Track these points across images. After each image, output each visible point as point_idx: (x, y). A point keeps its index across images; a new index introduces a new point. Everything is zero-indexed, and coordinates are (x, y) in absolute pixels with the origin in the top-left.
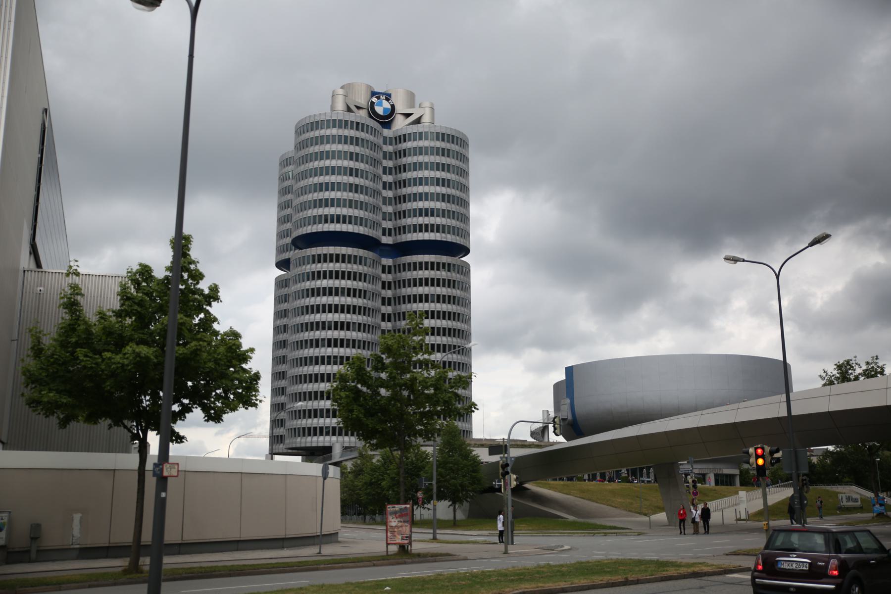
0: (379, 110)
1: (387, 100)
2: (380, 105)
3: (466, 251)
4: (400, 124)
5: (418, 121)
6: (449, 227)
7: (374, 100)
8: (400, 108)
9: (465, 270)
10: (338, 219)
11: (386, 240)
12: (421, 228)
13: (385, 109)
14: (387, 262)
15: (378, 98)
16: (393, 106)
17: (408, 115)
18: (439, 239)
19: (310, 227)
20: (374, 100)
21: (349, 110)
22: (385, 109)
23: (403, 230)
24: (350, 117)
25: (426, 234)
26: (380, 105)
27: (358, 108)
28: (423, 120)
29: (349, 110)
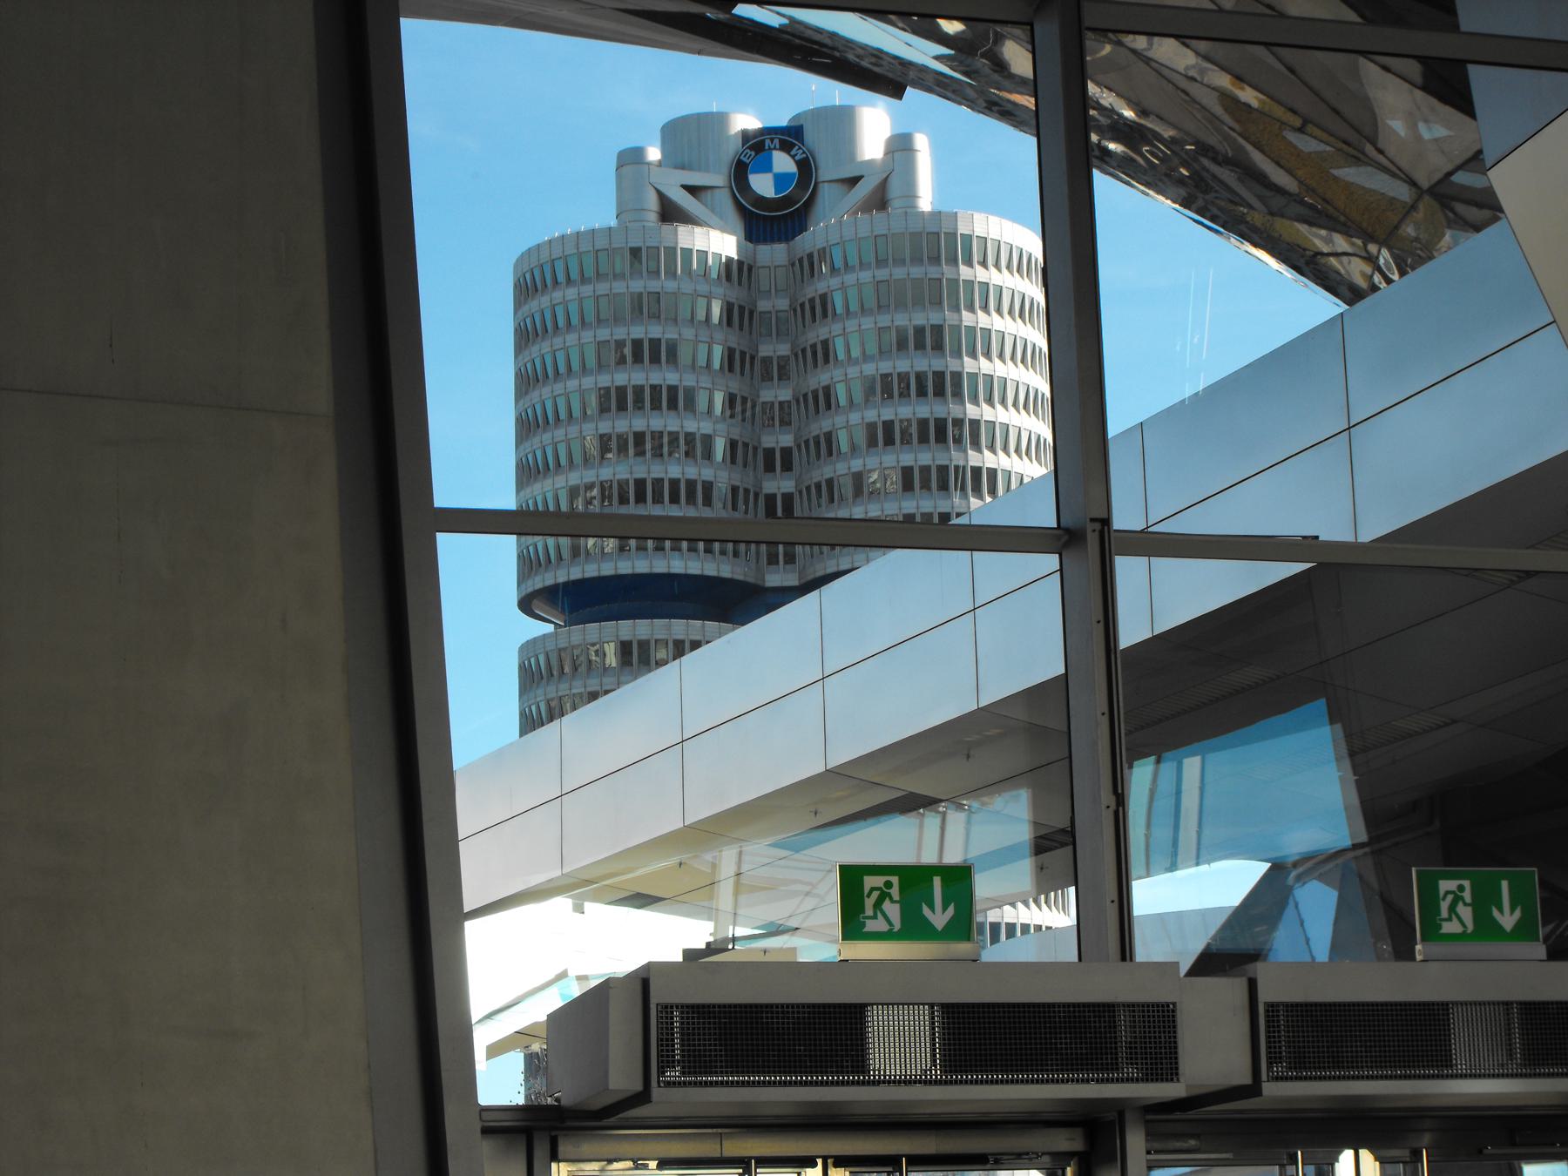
0: (762, 185)
1: (786, 147)
2: (767, 167)
8: (827, 170)
13: (780, 180)
16: (806, 167)
17: (853, 181)
22: (780, 180)
26: (767, 167)
27: (693, 190)
28: (894, 190)
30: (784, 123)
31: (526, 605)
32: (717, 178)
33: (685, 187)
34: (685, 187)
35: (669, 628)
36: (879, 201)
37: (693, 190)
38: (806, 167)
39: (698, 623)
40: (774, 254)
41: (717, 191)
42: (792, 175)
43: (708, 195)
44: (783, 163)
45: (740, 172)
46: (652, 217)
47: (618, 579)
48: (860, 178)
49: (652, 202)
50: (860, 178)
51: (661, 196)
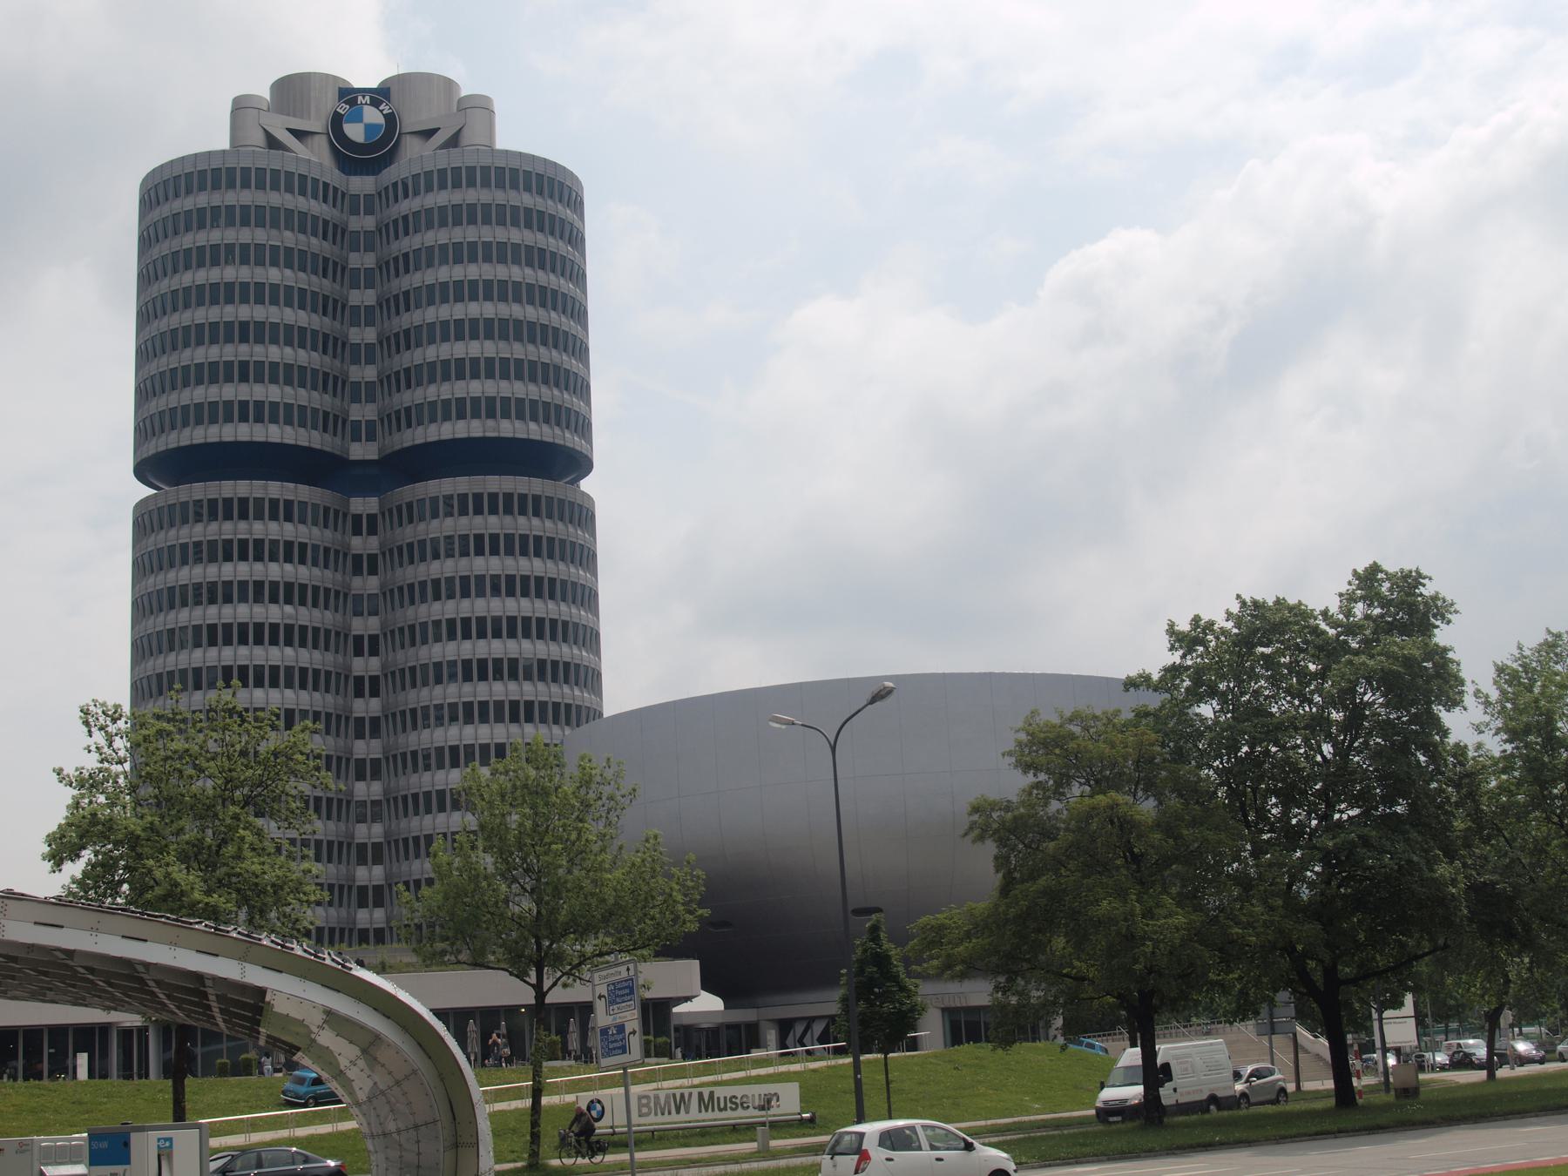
0: (355, 132)
1: (375, 103)
3: (580, 464)
4: (415, 156)
5: (454, 141)
6: (533, 403)
7: (343, 109)
8: (412, 120)
9: (582, 514)
10: (245, 411)
11: (361, 451)
14: (364, 505)
15: (352, 102)
17: (428, 134)
18: (479, 434)
19: (174, 435)
20: (343, 109)
21: (273, 143)
22: (370, 128)
24: (274, 161)
25: (461, 424)
27: (299, 135)
28: (466, 139)
30: (373, 84)
31: (144, 471)
32: (316, 123)
33: (291, 131)
34: (291, 131)
35: (266, 488)
36: (454, 141)
37: (299, 135)
38: (391, 119)
39: (291, 485)
40: (362, 185)
41: (317, 137)
42: (379, 126)
43: (309, 140)
44: (373, 116)
45: (337, 121)
47: (221, 445)
48: (435, 131)
49: (259, 139)
50: (435, 131)
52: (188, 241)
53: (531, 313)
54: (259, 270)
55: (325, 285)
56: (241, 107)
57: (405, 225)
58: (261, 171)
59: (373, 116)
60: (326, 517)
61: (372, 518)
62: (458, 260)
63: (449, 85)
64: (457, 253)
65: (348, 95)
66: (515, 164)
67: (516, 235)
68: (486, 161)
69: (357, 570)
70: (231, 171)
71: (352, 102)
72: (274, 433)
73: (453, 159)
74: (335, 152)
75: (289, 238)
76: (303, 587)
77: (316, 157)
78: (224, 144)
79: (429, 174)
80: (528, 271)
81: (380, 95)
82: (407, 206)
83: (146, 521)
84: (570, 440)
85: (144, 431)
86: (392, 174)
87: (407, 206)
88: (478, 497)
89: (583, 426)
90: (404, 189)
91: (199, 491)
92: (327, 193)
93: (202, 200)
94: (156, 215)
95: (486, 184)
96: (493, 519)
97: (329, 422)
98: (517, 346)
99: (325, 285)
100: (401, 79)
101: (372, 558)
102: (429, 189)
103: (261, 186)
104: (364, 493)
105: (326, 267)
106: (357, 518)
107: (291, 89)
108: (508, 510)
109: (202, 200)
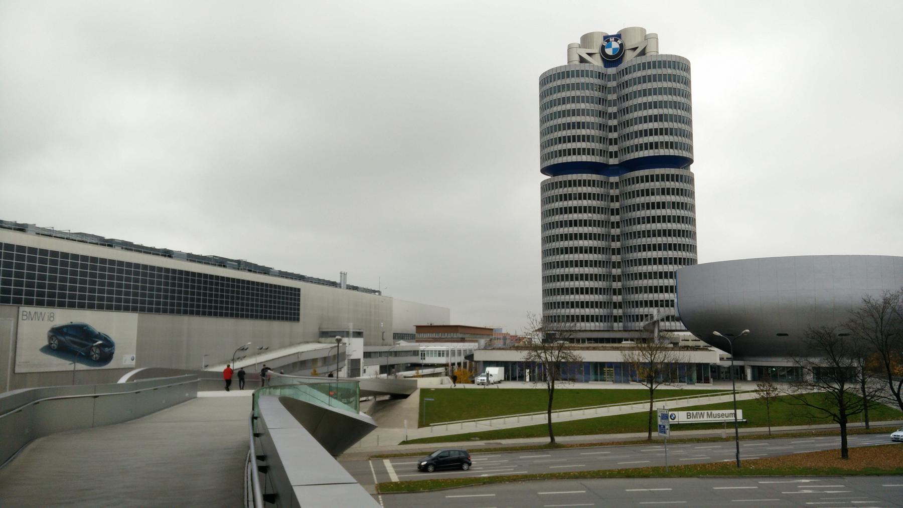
0: (609, 51)
1: (616, 40)
2: (610, 46)
3: (689, 161)
4: (630, 58)
5: (643, 53)
7: (605, 44)
8: (629, 45)
9: (690, 180)
11: (613, 161)
12: (640, 147)
14: (614, 179)
17: (635, 49)
21: (582, 60)
23: (628, 150)
26: (610, 46)
27: (590, 54)
28: (647, 50)
29: (582, 60)
30: (615, 33)
32: (596, 50)
36: (643, 53)
37: (590, 54)
38: (621, 45)
40: (612, 71)
45: (603, 48)
46: (577, 63)
47: (567, 163)
49: (577, 58)
51: (580, 56)
52: (555, 96)
53: (670, 111)
54: (578, 105)
55: (600, 107)
56: (570, 48)
57: (626, 84)
58: (578, 71)
59: (615, 45)
60: (601, 184)
61: (617, 183)
62: (645, 95)
63: (643, 30)
64: (645, 93)
65: (607, 38)
66: (664, 59)
67: (666, 84)
68: (654, 59)
69: (612, 201)
70: (568, 72)
71: (608, 41)
72: (584, 158)
73: (643, 59)
74: (603, 60)
75: (587, 93)
76: (594, 207)
77: (597, 63)
78: (565, 62)
79: (634, 66)
80: (670, 96)
81: (618, 37)
82: (627, 78)
83: (545, 187)
84: (685, 154)
85: (543, 158)
86: (622, 66)
87: (627, 78)
88: (652, 176)
89: (690, 148)
90: (626, 71)
91: (561, 178)
92: (600, 75)
93: (559, 82)
94: (545, 88)
95: (654, 67)
96: (657, 183)
97: (602, 153)
98: (666, 123)
99: (600, 107)
100: (625, 30)
101: (617, 196)
102: (634, 71)
103: (578, 76)
104: (614, 175)
105: (601, 101)
106: (612, 183)
107: (586, 39)
108: (663, 180)
109: (559, 82)
